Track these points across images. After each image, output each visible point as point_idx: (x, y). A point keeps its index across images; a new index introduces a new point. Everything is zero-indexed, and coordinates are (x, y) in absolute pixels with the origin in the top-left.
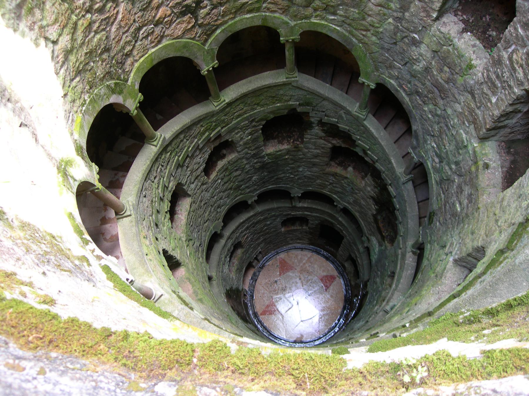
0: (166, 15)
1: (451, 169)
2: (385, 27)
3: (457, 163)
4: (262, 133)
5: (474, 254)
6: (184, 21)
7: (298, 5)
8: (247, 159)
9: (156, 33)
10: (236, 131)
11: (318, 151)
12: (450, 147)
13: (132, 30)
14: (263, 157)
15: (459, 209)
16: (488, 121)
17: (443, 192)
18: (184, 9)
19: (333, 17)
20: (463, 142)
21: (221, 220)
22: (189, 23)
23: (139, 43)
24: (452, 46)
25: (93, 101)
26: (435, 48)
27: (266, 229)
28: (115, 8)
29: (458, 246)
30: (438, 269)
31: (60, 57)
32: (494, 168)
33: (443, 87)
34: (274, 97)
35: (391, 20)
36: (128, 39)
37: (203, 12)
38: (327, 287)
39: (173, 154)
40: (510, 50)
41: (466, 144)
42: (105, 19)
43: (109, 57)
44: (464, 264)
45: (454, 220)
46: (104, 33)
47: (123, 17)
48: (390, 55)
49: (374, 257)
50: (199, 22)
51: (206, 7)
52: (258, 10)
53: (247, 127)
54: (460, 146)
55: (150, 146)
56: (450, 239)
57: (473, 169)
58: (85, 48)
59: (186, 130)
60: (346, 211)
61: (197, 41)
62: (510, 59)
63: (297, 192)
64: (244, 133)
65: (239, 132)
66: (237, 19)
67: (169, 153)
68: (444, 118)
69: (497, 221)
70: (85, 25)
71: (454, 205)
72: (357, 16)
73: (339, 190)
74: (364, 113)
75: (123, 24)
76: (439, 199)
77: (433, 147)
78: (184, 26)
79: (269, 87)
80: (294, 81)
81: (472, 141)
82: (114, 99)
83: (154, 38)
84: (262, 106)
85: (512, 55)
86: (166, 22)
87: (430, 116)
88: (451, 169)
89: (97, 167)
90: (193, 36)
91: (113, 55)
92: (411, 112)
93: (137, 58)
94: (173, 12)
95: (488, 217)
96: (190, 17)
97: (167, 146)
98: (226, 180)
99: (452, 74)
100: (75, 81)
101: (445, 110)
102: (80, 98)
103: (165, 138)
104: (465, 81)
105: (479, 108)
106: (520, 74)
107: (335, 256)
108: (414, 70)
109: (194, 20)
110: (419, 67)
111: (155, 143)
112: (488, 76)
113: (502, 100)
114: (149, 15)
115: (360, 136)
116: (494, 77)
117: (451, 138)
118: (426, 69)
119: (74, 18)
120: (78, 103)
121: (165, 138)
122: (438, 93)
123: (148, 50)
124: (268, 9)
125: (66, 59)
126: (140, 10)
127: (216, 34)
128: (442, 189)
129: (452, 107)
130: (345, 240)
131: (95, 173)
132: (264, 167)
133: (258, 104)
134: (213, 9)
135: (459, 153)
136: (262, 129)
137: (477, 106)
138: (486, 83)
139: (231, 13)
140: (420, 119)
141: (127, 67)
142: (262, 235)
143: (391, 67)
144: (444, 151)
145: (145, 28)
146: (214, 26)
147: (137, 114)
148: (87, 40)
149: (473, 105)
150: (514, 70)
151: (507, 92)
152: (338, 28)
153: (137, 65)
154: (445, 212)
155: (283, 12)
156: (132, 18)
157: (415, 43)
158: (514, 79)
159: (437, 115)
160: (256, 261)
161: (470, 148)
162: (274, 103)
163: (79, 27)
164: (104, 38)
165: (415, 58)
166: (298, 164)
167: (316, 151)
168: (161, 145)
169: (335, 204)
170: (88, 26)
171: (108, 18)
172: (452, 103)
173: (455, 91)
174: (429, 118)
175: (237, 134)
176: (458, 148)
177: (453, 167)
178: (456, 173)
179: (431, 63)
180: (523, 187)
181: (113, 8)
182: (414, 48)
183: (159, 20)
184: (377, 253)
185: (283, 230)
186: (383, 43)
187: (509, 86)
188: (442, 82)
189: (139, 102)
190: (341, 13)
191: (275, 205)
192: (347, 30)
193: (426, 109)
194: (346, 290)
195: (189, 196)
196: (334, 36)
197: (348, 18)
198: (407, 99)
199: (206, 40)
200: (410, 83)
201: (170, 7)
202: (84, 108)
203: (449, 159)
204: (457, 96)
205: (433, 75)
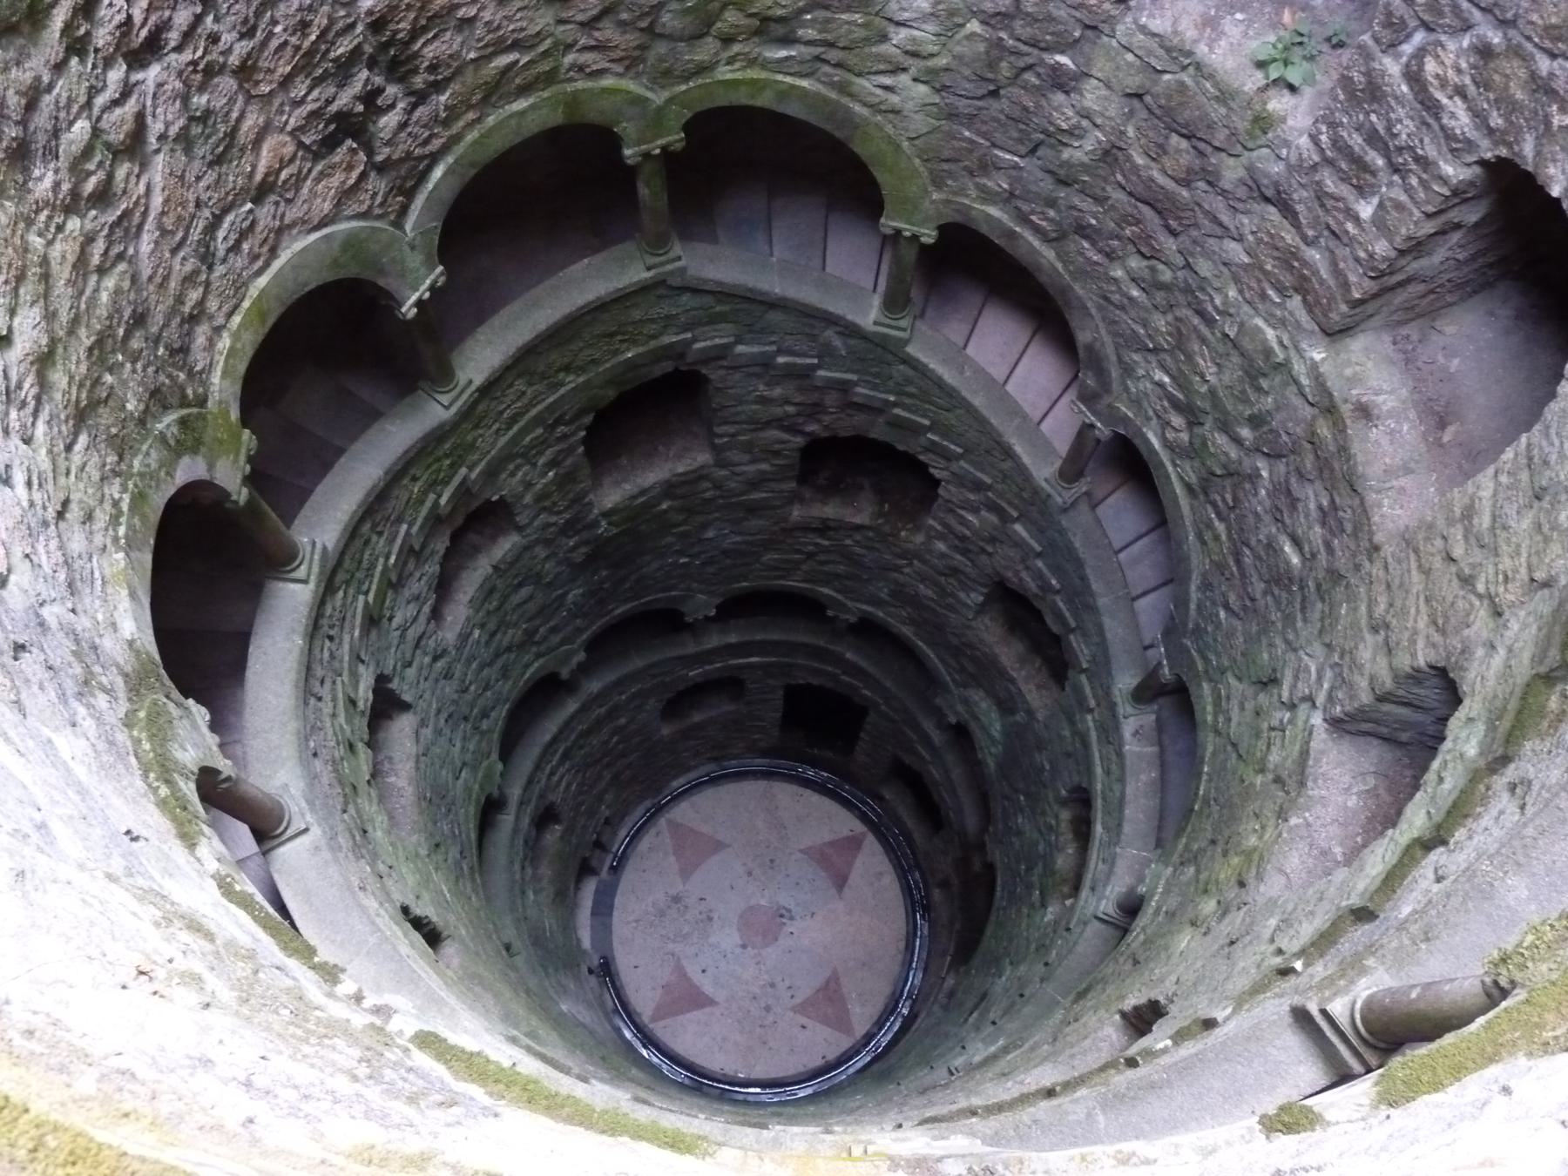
0: (281, 160)
1: (1237, 441)
2: (958, 49)
3: (1256, 421)
4: (588, 453)
5: (1401, 692)
6: (333, 167)
7: (670, 37)
8: (547, 543)
9: (262, 224)
10: (511, 467)
11: (764, 466)
12: (1213, 374)
13: (195, 235)
15: (1295, 560)
16: (1353, 278)
17: (1218, 514)
18: (332, 127)
19: (783, 53)
20: (1268, 352)
21: (495, 756)
23: (220, 270)
24: (1191, 70)
25: (139, 499)
26: (1134, 82)
27: (618, 743)
28: (138, 176)
29: (1329, 674)
30: (1274, 757)
31: (26, 385)
32: (1391, 414)
33: (1170, 196)
34: (612, 335)
35: (974, 26)
36: (188, 267)
37: (389, 121)
38: (840, 881)
39: (351, 591)
40: (1407, 49)
42: (121, 218)
43: (147, 339)
44: (1366, 727)
45: (1284, 595)
46: (122, 267)
47: (167, 201)
48: (979, 133)
49: (990, 756)
50: (379, 158)
51: (392, 106)
52: (550, 78)
53: (541, 445)
54: (1260, 368)
55: (281, 584)
56: (1291, 656)
57: (1324, 430)
58: (83, 332)
59: (374, 509)
60: (868, 630)
61: (379, 217)
62: (1414, 76)
63: (702, 605)
64: (534, 465)
65: (518, 468)
66: (491, 120)
67: (341, 593)
68: (1192, 293)
69: (1467, 581)
70: (71, 258)
71: (1272, 547)
72: (860, 33)
73: (841, 569)
74: (903, 323)
75: (168, 222)
76: (1208, 536)
77: (1160, 385)
78: (335, 181)
79: (600, 308)
80: (672, 273)
81: (1304, 345)
82: (189, 470)
83: (257, 243)
84: (582, 370)
85: (1421, 65)
86: (285, 182)
87: (1135, 293)
88: (1237, 441)
89: (203, 710)
90: (364, 207)
91: (154, 329)
92: (1066, 290)
93: (220, 321)
94: (300, 145)
95: (1426, 572)
96: (353, 151)
97: (334, 572)
98: (492, 626)
99: (1202, 154)
100: (78, 447)
101: (1188, 266)
102: (102, 501)
103: (325, 548)
104: (1250, 169)
105: (1310, 243)
106: (1460, 118)
107: (846, 776)
108: (1067, 164)
109: (362, 156)
110: (1080, 152)
111: (301, 572)
112: (1336, 142)
113: (1399, 206)
114: (234, 176)
115: (896, 394)
116: (1356, 141)
117: (1221, 348)
118: (1106, 153)
119: (36, 241)
120: (102, 518)
121: (325, 548)
122: (1157, 220)
123: (246, 285)
124: (581, 69)
125: (43, 383)
126: (211, 165)
127: (430, 186)
128: (1214, 505)
129: (1208, 255)
130: (871, 718)
131: (205, 730)
132: (599, 553)
133: (567, 369)
134: (414, 106)
135: (1259, 389)
136: (584, 441)
137: (1304, 238)
138: (1330, 162)
139: (470, 107)
140: (1100, 308)
141: (199, 359)
142: (608, 765)
143: (986, 166)
144: (1204, 389)
145: (229, 218)
146: (421, 158)
147: (250, 502)
148: (83, 306)
149: (1290, 237)
150: (1434, 108)
151: (1414, 181)
152: (804, 83)
153: (225, 342)
154: (1243, 575)
155: (627, 68)
156: (192, 197)
157: (1061, 81)
158: (1434, 138)
159: (1162, 286)
160: (598, 852)
161: (1299, 368)
162: (616, 352)
163: (55, 267)
164: (126, 284)
165: (1064, 126)
166: (699, 519)
167: (752, 468)
168: (321, 573)
169: (830, 613)
170: (79, 259)
171: (127, 214)
172: (1211, 241)
173: (1218, 205)
174: (1131, 299)
175: (513, 474)
176: (1253, 375)
177: (1245, 433)
178: (1258, 450)
179: (1123, 133)
180: (1546, 463)
181: (133, 179)
182: (1059, 97)
183: (264, 180)
184: (997, 735)
185: (666, 731)
186: (952, 99)
187: (1424, 162)
188: (1170, 185)
189: (250, 460)
190: (811, 33)
191: (637, 663)
192: (832, 85)
193: (1119, 273)
195: (406, 707)
196: (793, 109)
197: (831, 45)
198: (1049, 254)
199: (404, 210)
200: (1052, 203)
201: (291, 133)
202: (122, 531)
204: (1225, 218)
205: (1135, 168)
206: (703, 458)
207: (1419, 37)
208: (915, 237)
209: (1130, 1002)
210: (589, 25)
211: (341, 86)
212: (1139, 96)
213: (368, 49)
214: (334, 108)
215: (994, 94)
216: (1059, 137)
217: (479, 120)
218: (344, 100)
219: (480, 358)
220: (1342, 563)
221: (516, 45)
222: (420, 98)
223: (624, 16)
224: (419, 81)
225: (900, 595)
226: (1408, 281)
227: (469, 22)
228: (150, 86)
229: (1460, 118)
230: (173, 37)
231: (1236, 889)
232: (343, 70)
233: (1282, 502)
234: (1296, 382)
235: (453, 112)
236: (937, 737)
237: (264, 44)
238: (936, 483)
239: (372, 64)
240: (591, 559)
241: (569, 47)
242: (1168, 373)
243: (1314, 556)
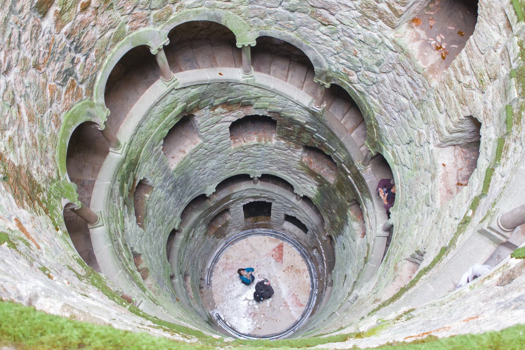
1: (375, 72)
3: (378, 64)
10: (144, 166)
17: (375, 97)
18: (65, 75)
41: (380, 41)
60: (266, 178)
66: (109, 56)
73: (252, 161)
88: (375, 72)
101: (341, 23)
117: (359, 45)
128: (372, 95)
130: (274, 205)
134: (86, 59)
136: (163, 150)
155: (146, 23)
161: (387, 42)
167: (215, 139)
169: (251, 177)
193: (318, 33)
194: (299, 250)
203: (367, 64)
206: (200, 141)
208: (249, 45)
214: (64, 69)
218: (67, 65)
219: (125, 133)
220: (425, 97)
221: (111, 28)
222: (87, 56)
223: (142, 6)
225: (273, 162)
228: (12, 81)
230: (13, 63)
231: (427, 208)
233: (396, 85)
236: (299, 203)
237: (39, 55)
240: (175, 187)
243: (412, 98)
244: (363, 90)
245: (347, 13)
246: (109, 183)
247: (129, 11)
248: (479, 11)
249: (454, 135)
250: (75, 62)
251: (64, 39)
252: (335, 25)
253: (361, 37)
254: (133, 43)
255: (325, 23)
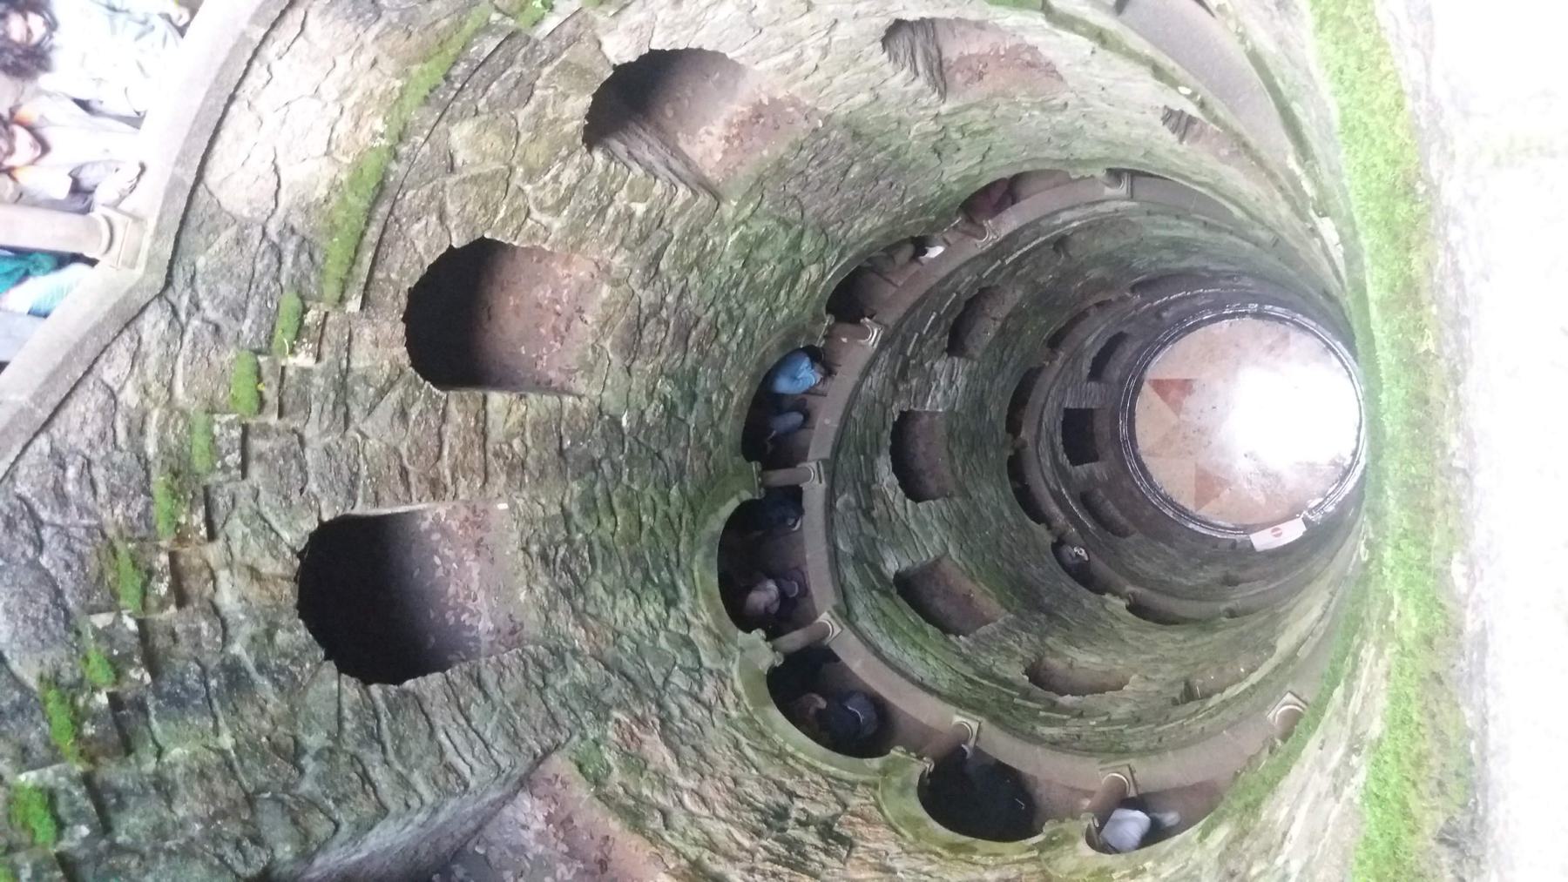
14: (1017, 613)
22: (851, 823)
37: (816, 811)
51: (803, 810)
62: (557, 210)
78: (863, 829)
88: (801, 234)
96: (841, 824)
113: (631, 188)
117: (752, 266)
124: (737, 705)
130: (1068, 404)
139: (786, 763)
144: (779, 267)
150: (572, 189)
161: (747, 211)
182: (648, 418)
190: (665, 574)
193: (734, 346)
200: (708, 401)
203: (789, 249)
207: (535, 214)
209: (1173, 138)
210: (710, 708)
211: (803, 844)
212: (629, 369)
213: (774, 834)
214: (820, 844)
215: (659, 455)
216: (670, 410)
217: (793, 757)
218: (810, 837)
221: (737, 745)
222: (792, 795)
223: (696, 688)
224: (783, 800)
226: (671, 170)
227: (735, 781)
229: (569, 176)
232: (793, 844)
234: (753, 211)
235: (793, 772)
238: (902, 413)
239: (783, 830)
240: (1041, 609)
241: (727, 716)
242: (778, 294)
243: (850, 157)
244: (836, 252)
245: (694, 293)
246: (1039, 749)
247: (706, 713)
248: (681, 47)
249: (920, 69)
250: (804, 818)
251: (764, 842)
252: (717, 314)
253: (738, 265)
254: (765, 704)
255: (715, 330)
